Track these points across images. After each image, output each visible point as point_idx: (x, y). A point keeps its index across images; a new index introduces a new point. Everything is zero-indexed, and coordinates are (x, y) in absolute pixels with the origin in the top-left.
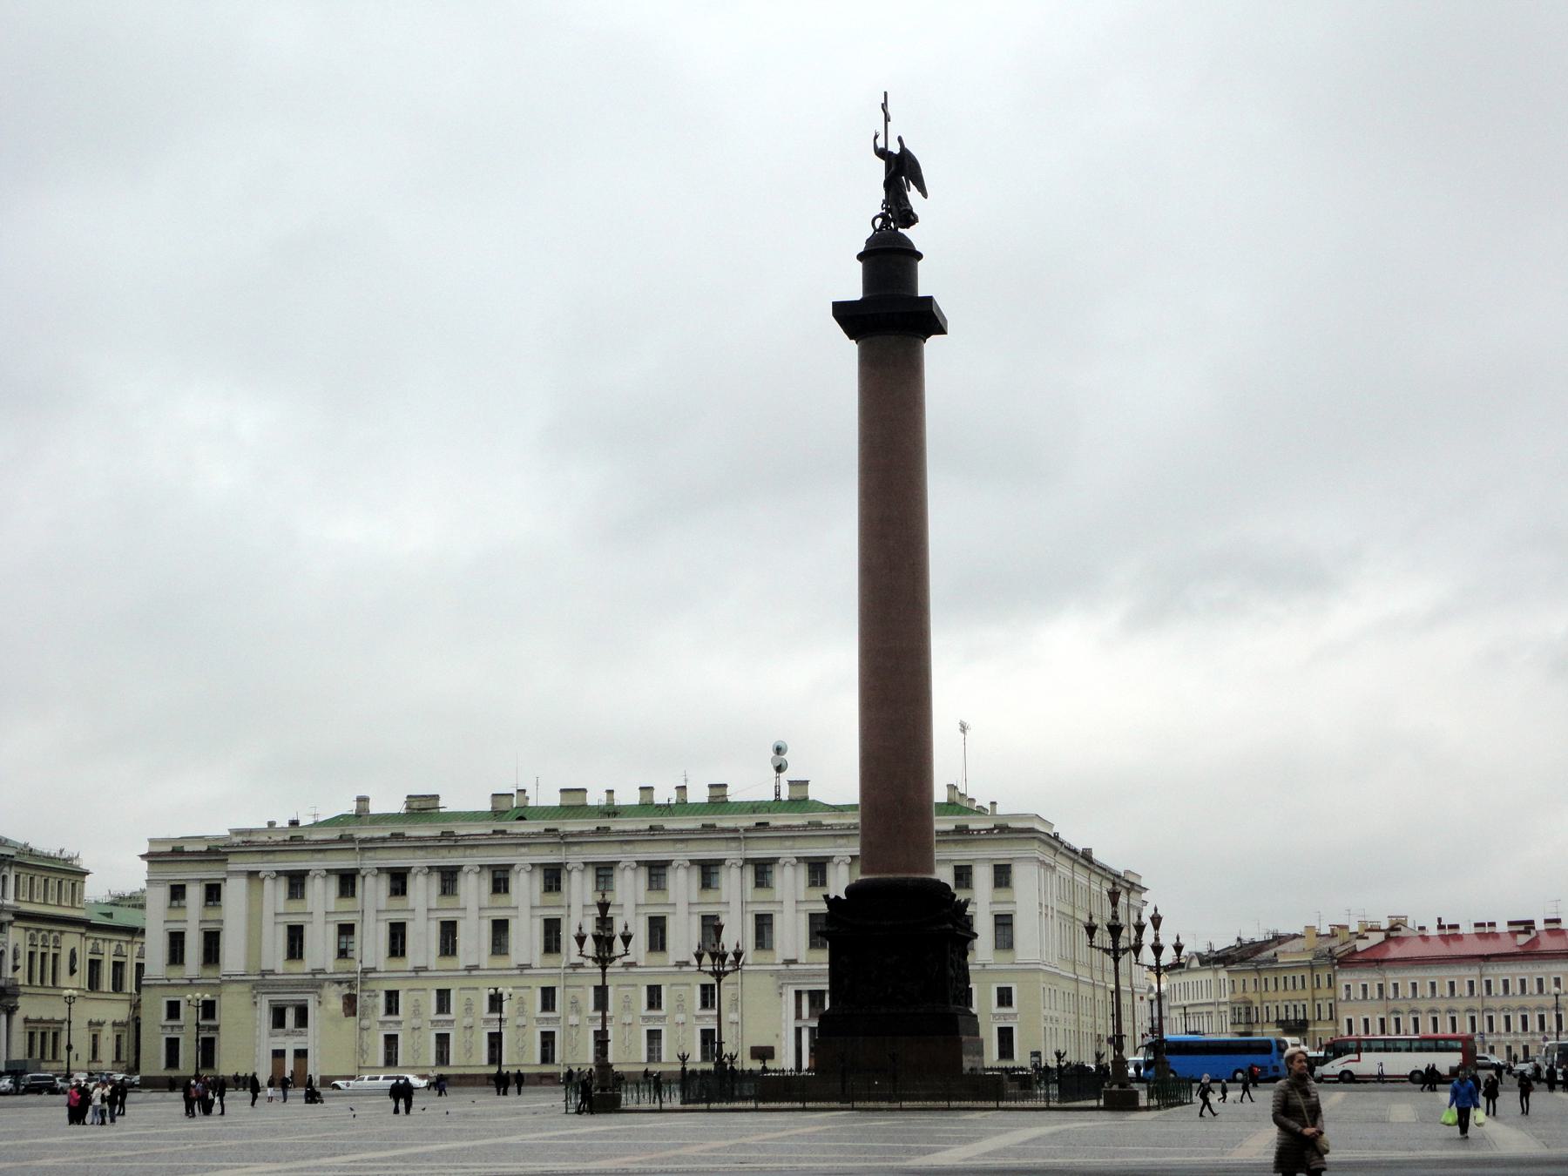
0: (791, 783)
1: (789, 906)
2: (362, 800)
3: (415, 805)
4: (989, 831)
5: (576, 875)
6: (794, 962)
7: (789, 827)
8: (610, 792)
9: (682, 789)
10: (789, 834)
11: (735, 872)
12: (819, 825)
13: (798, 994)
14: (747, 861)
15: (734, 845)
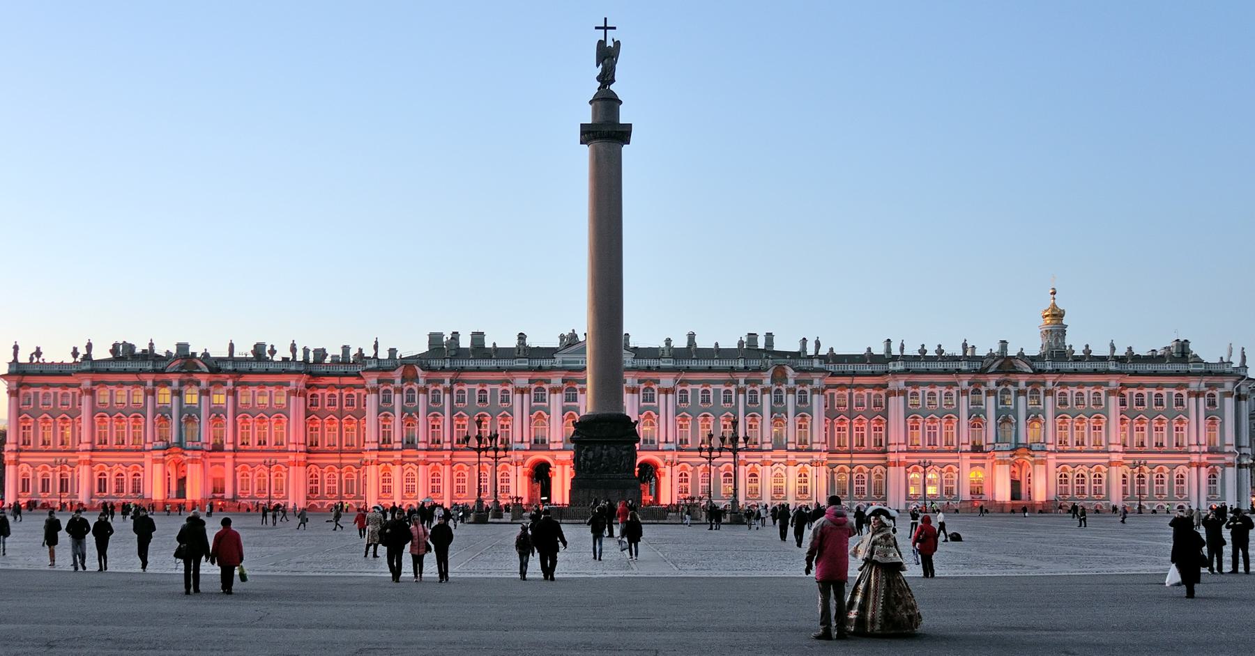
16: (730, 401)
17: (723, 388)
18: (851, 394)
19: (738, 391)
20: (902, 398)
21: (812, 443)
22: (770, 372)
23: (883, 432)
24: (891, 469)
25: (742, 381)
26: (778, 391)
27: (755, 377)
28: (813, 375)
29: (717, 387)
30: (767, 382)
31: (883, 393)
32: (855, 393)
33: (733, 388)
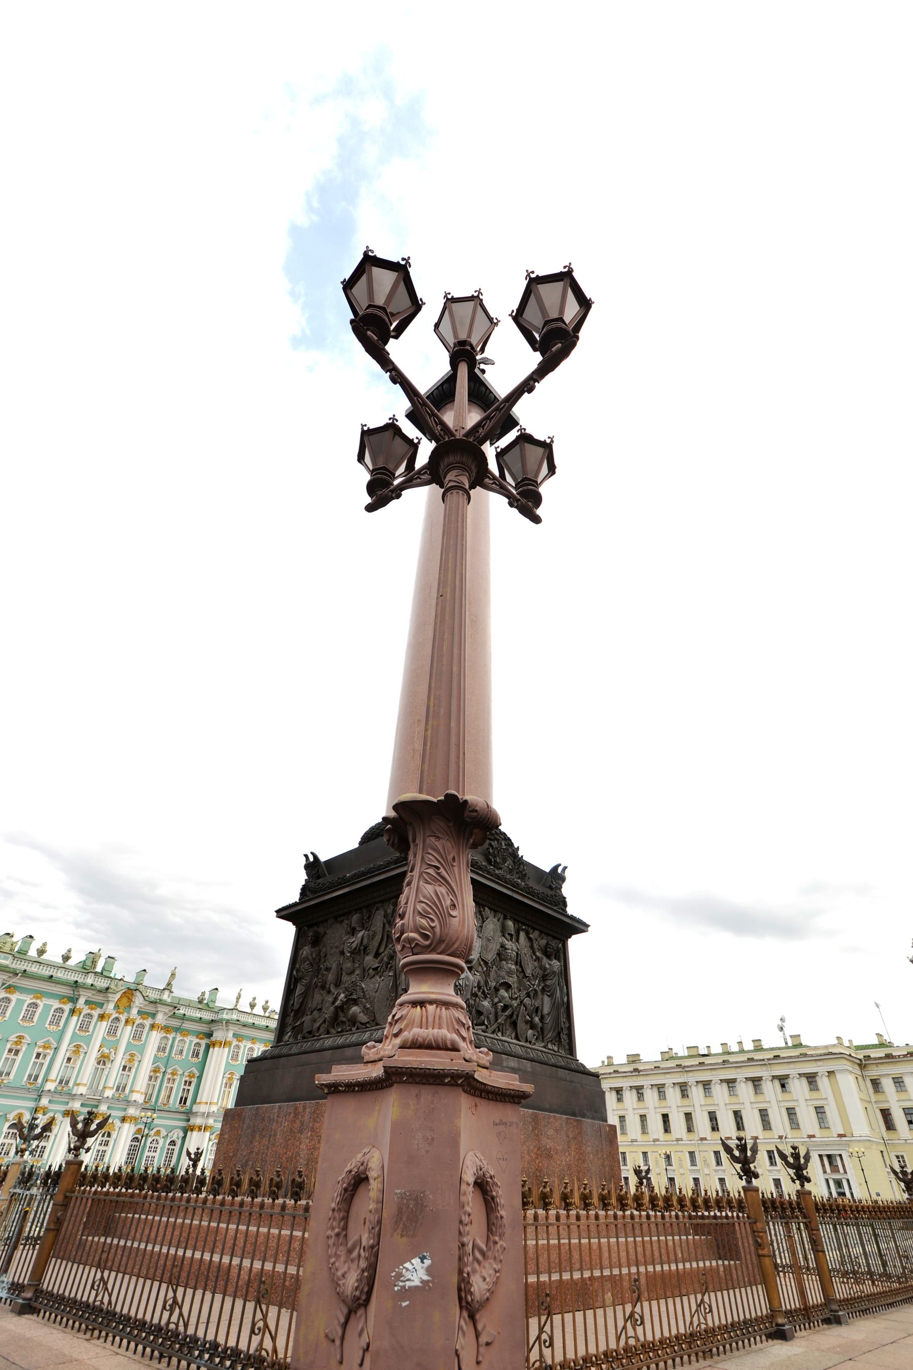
0: (791, 1036)
1: (802, 1102)
2: (609, 1058)
3: (630, 1059)
4: (905, 1056)
5: (694, 1088)
6: (813, 1136)
7: (791, 1057)
8: (708, 1047)
9: (740, 1043)
10: (791, 1061)
11: (769, 1084)
12: (805, 1055)
13: (821, 1156)
14: (774, 1077)
15: (764, 1068)
16: (58, 1024)
17: (56, 1004)
18: (174, 1039)
19: (73, 1012)
20: (227, 1049)
21: (132, 1091)
22: (118, 996)
23: (192, 1088)
24: (195, 1133)
25: (82, 1001)
26: (117, 1019)
27: (99, 998)
28: (161, 1008)
29: (50, 1002)
30: (111, 1006)
31: (203, 1042)
32: (179, 1038)
33: (67, 1007)
